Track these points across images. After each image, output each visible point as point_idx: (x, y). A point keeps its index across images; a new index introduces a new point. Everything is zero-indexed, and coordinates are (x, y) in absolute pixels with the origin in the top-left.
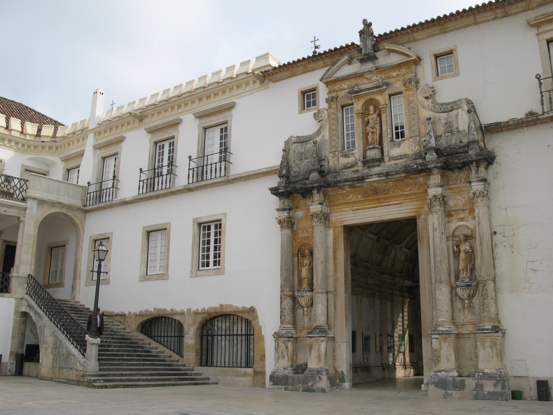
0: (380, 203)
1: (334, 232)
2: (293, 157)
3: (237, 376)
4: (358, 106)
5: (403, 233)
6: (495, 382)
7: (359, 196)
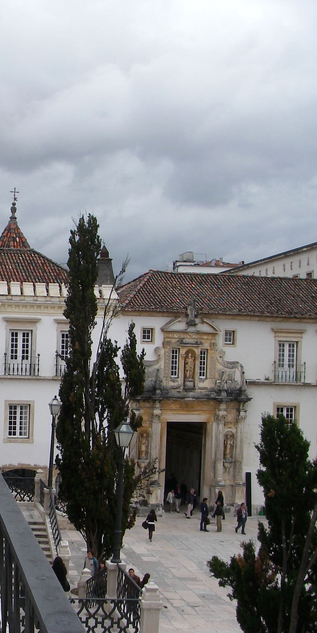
1: (161, 425)
4: (183, 351)
5: (198, 430)
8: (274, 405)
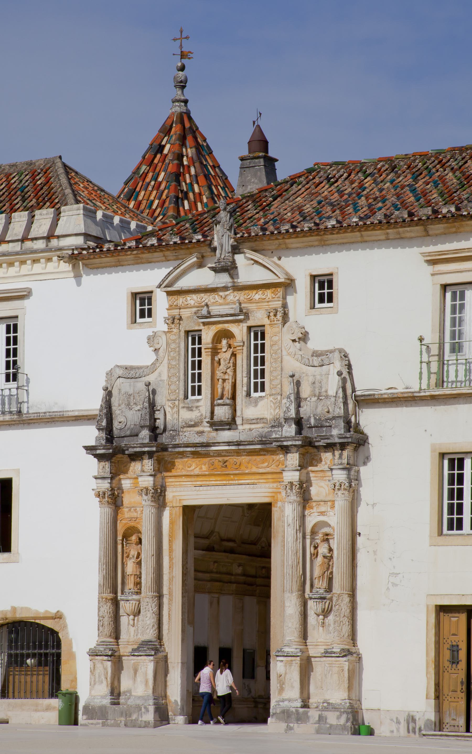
0: (229, 480)
1: (171, 514)
2: (117, 399)
3: (36, 711)
4: (208, 336)
6: (338, 713)
7: (203, 467)
8: (433, 451)
